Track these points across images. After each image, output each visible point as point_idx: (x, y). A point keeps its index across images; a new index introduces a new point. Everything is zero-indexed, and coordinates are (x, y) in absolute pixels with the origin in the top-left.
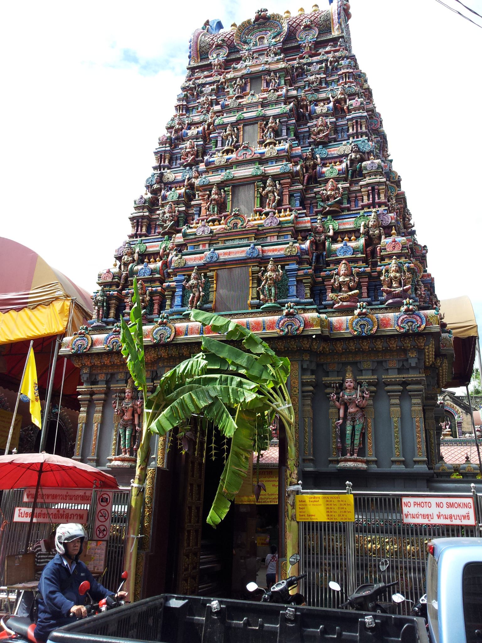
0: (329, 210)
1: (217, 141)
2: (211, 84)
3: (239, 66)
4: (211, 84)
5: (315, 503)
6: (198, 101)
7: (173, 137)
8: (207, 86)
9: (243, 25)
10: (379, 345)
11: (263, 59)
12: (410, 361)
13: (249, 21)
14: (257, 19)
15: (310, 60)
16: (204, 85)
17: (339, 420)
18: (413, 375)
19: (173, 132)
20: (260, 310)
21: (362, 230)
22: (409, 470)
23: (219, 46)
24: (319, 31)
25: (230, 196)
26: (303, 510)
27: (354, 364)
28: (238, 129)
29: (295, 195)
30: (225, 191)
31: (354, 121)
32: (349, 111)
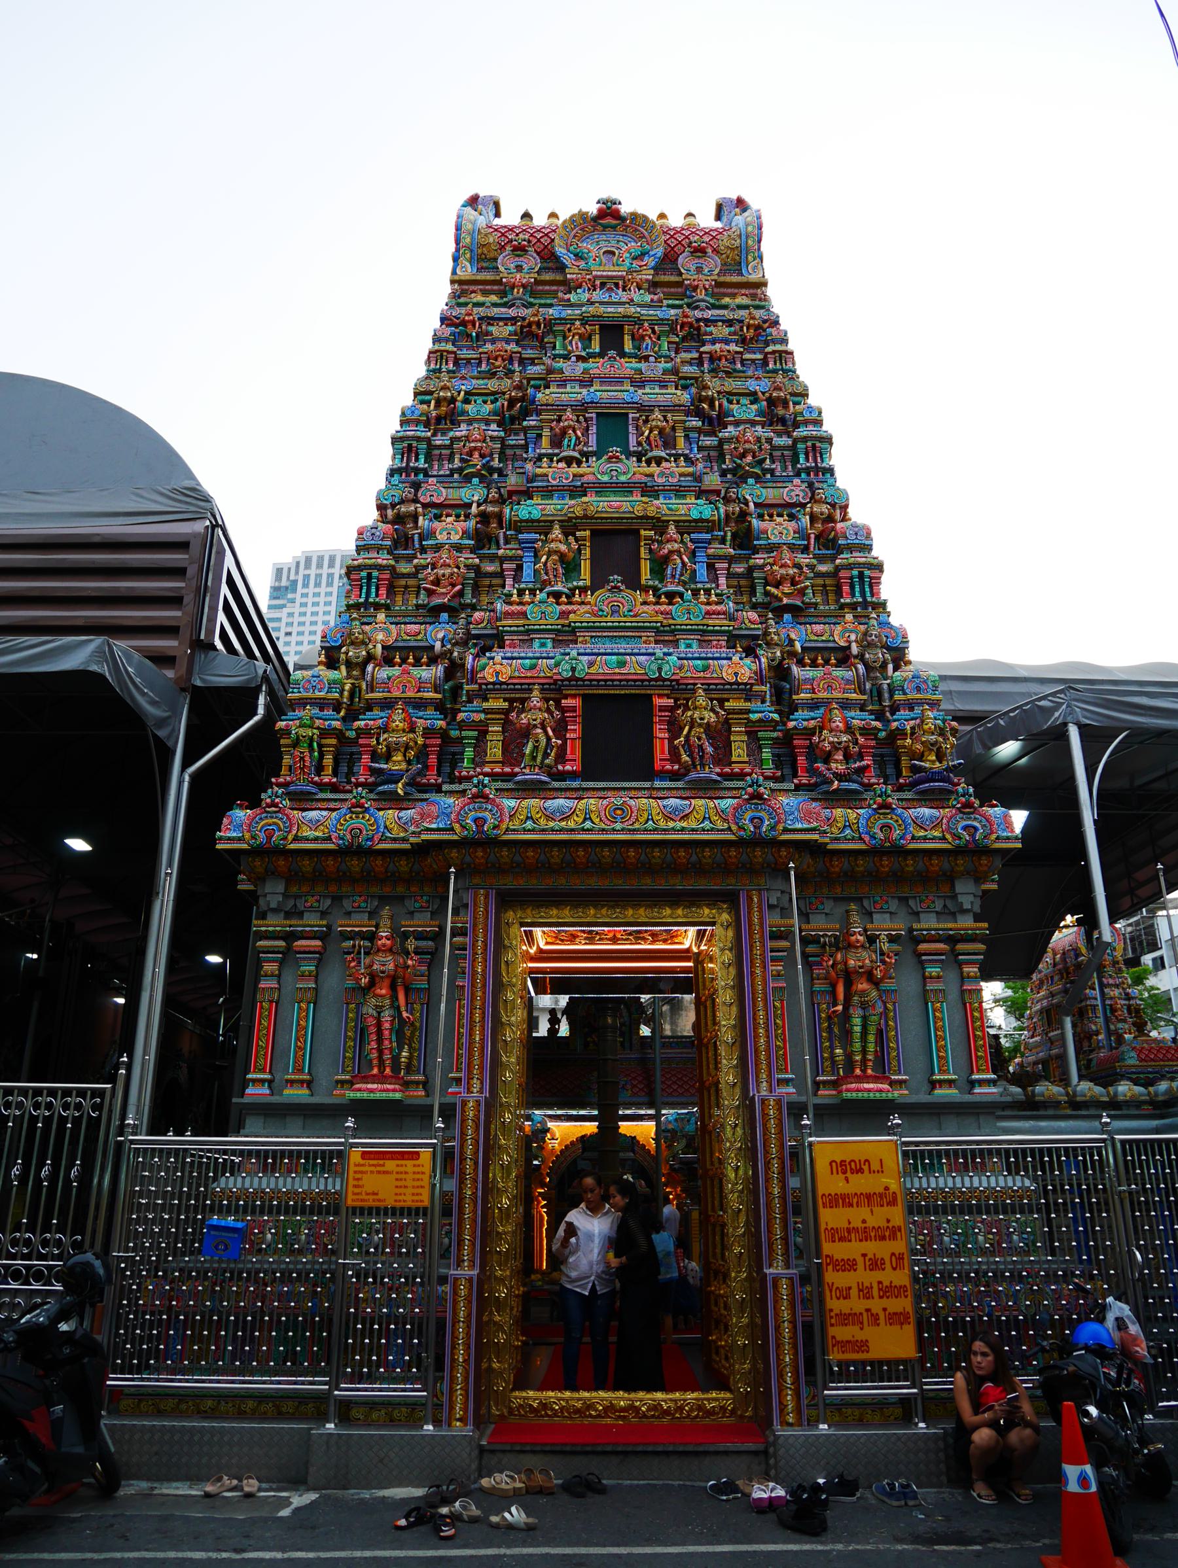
0: (786, 605)
1: (540, 436)
2: (507, 320)
3: (573, 297)
4: (507, 320)
5: (379, 1169)
6: (481, 350)
7: (434, 414)
8: (501, 324)
9: (572, 219)
10: (910, 865)
11: (621, 295)
12: (961, 899)
13: (582, 215)
14: (602, 214)
15: (709, 314)
16: (491, 320)
17: (835, 1005)
18: (966, 923)
19: (433, 402)
20: (680, 784)
21: (855, 649)
22: (967, 1098)
23: (519, 250)
24: (724, 264)
25: (588, 549)
26: (360, 1183)
27: (859, 900)
28: (586, 420)
29: (717, 565)
30: (577, 540)
31: (809, 444)
32: (796, 425)
